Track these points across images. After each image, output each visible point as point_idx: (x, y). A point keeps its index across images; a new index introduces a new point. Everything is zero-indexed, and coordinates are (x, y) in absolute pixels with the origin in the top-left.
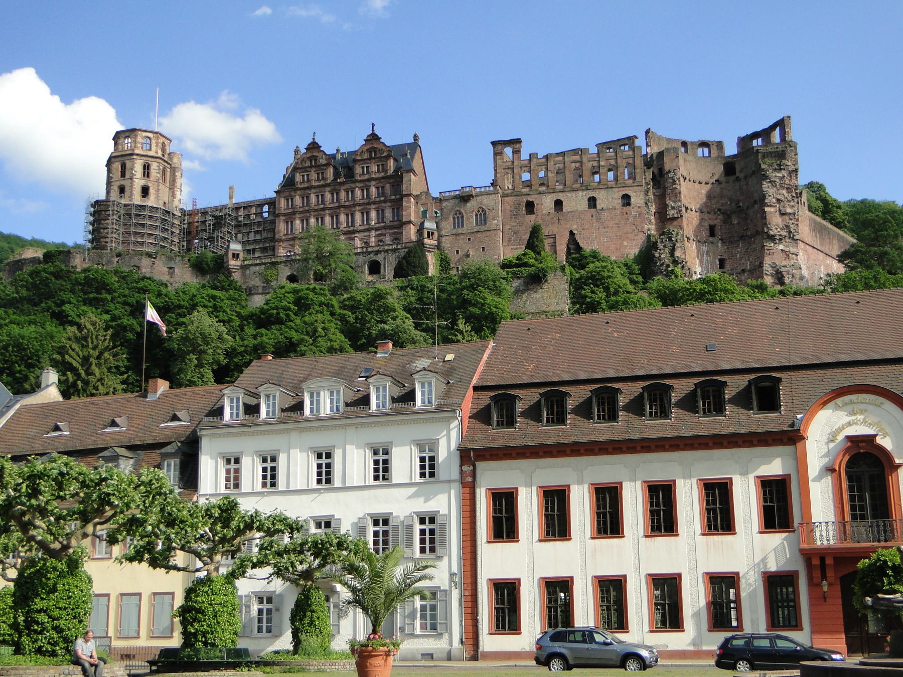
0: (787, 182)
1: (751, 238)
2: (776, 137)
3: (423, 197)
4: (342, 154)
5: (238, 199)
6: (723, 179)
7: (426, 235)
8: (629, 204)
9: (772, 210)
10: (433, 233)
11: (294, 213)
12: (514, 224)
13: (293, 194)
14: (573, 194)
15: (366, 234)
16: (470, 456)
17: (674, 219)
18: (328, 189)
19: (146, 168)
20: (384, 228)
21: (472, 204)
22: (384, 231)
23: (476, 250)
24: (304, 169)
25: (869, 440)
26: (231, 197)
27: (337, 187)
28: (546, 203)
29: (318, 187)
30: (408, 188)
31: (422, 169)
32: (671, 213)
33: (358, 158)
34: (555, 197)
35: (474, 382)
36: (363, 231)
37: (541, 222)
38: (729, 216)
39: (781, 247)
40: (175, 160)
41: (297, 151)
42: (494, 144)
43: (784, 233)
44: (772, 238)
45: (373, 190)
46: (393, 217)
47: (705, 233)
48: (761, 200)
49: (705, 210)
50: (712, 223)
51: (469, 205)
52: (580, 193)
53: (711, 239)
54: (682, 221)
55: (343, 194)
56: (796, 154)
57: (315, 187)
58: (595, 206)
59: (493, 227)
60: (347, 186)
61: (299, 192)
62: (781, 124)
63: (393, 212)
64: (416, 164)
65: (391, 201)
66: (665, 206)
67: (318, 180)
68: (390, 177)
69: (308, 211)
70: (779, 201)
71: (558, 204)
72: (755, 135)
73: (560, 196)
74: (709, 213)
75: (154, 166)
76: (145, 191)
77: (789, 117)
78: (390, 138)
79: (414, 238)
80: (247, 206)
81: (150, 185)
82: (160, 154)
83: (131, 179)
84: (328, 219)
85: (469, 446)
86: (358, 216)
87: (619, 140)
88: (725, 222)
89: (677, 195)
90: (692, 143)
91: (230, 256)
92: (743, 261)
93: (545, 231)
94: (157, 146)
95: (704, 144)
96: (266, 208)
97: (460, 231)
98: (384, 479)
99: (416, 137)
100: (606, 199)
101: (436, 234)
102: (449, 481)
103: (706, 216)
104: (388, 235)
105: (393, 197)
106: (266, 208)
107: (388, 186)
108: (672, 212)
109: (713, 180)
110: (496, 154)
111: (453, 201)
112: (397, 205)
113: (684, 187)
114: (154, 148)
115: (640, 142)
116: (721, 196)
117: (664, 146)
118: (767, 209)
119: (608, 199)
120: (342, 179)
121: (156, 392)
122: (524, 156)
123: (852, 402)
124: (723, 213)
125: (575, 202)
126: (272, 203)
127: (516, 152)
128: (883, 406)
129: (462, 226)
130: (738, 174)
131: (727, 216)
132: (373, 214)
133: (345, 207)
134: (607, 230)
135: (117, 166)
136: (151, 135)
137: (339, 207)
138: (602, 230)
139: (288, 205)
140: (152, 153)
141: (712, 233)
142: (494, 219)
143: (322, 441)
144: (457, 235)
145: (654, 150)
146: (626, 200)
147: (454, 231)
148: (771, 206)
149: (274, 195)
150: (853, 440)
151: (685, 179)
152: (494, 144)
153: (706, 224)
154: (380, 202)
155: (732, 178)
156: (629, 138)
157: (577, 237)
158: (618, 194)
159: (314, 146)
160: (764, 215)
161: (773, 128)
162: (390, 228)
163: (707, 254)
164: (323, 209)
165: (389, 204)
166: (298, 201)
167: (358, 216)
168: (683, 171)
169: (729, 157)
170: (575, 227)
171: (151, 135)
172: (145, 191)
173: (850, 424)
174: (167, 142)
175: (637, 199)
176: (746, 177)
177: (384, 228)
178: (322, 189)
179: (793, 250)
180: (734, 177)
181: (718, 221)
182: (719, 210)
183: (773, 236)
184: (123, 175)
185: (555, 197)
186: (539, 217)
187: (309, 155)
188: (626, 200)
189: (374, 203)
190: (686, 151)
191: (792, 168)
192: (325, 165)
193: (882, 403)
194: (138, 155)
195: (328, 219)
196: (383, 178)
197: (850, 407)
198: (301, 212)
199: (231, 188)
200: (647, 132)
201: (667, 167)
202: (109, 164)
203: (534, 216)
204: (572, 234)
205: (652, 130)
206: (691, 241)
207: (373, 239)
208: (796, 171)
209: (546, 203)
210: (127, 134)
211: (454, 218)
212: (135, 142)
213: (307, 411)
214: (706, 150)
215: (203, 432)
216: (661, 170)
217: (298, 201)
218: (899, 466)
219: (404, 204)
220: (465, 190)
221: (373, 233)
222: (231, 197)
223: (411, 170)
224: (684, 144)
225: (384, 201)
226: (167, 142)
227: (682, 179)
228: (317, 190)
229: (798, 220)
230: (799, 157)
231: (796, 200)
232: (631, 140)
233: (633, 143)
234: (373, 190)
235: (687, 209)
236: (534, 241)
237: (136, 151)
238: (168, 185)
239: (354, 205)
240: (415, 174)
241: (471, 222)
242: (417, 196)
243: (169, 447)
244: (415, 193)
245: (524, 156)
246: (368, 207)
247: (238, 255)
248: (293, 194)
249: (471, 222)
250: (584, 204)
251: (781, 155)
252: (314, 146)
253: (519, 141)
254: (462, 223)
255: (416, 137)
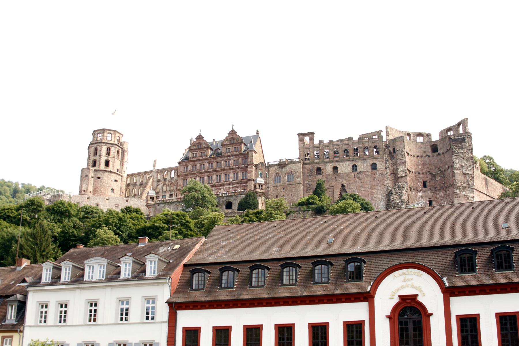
0: (467, 156)
1: (446, 188)
2: (461, 131)
3: (260, 165)
4: (216, 142)
5: (159, 167)
6: (430, 154)
7: (258, 187)
8: (376, 169)
9: (458, 172)
10: (262, 186)
11: (187, 175)
12: (309, 180)
13: (188, 164)
14: (344, 163)
15: (227, 186)
16: (174, 307)
17: (402, 177)
18: (206, 161)
19: (108, 150)
20: (238, 183)
21: (286, 169)
22: (237, 185)
23: (288, 195)
24: (194, 150)
25: (413, 298)
26: (154, 166)
27: (212, 160)
28: (328, 168)
29: (202, 160)
30: (252, 160)
31: (261, 150)
32: (400, 173)
33: (225, 143)
34: (333, 165)
35: (185, 261)
36: (227, 185)
37: (325, 179)
38: (434, 176)
39: (464, 193)
40: (125, 146)
41: (191, 140)
42: (299, 135)
43: (465, 185)
44: (458, 187)
45: (232, 161)
46: (243, 177)
47: (420, 185)
48: (452, 167)
49: (421, 172)
50: (425, 180)
51: (284, 170)
52: (348, 163)
53: (424, 189)
54: (407, 179)
55: (215, 164)
56: (471, 140)
57: (199, 160)
58: (356, 170)
59: (298, 182)
60: (218, 159)
61: (191, 163)
62: (463, 123)
63: (243, 174)
64: (256, 148)
65: (242, 168)
66: (397, 169)
67: (202, 156)
68: (242, 154)
69: (195, 174)
70: (462, 166)
71: (335, 169)
72: (449, 129)
73: (337, 164)
74: (423, 174)
75: (112, 149)
76: (107, 163)
77: (467, 119)
78: (242, 133)
79: (253, 187)
80: (161, 171)
81: (110, 159)
82: (116, 142)
83: (100, 156)
84: (206, 178)
85: (174, 300)
86: (223, 176)
87: (372, 133)
88: (432, 179)
89: (404, 163)
90: (414, 134)
91: (149, 198)
92: (443, 202)
93: (326, 185)
94: (115, 138)
95: (420, 135)
96: (173, 172)
97: (278, 184)
98: (126, 320)
99: (258, 132)
100: (362, 166)
101: (264, 187)
102: (161, 322)
103: (421, 176)
104: (239, 187)
105: (243, 166)
106: (173, 172)
107: (240, 159)
108: (401, 173)
109: (424, 155)
110: (300, 141)
111: (275, 168)
112: (245, 170)
113: (407, 159)
114: (113, 139)
115: (384, 134)
116: (430, 164)
117: (397, 135)
118: (455, 171)
119: (363, 166)
120: (215, 156)
121: (21, 266)
122: (316, 141)
123: (403, 274)
124: (431, 174)
125: (345, 167)
126: (176, 169)
127: (312, 139)
128: (422, 276)
129: (280, 182)
130: (439, 152)
131: (433, 176)
132: (232, 175)
133: (216, 171)
134: (363, 184)
135: (93, 149)
136: (112, 132)
137: (213, 171)
138: (361, 184)
139: (184, 170)
140: (112, 142)
141: (425, 185)
142: (298, 178)
143: (92, 295)
144: (277, 186)
145: (391, 138)
146: (374, 166)
147: (275, 185)
148: (457, 169)
149: (177, 165)
150: (403, 298)
151: (408, 154)
152: (299, 135)
153: (421, 180)
154: (236, 168)
155: (435, 154)
156: (378, 132)
157: (346, 188)
158: (369, 163)
159: (200, 137)
160: (454, 176)
161: (459, 124)
162: (241, 183)
163: (422, 198)
164: (204, 173)
165: (240, 170)
166: (190, 168)
167: (223, 176)
168: (407, 149)
169: (434, 142)
170: (345, 182)
171: (112, 132)
172: (107, 163)
173: (402, 287)
174: (120, 136)
175: (380, 166)
176: (443, 153)
177: (238, 183)
178: (204, 161)
179: (471, 195)
180: (437, 153)
181: (428, 179)
182: (429, 172)
183: (459, 186)
184: (96, 154)
185: (333, 165)
186: (324, 177)
187: (197, 142)
188: (374, 166)
189: (232, 169)
190: (410, 139)
191: (469, 148)
192: (205, 148)
193: (421, 275)
194: (104, 143)
195: (206, 178)
196: (238, 155)
197: (402, 277)
198: (191, 174)
199: (155, 161)
200: (387, 128)
201: (398, 148)
202: (89, 148)
203: (321, 176)
204: (343, 186)
205: (390, 126)
206: (412, 190)
207: (231, 189)
208: (472, 149)
209: (328, 168)
210: (99, 132)
211: (275, 177)
212: (103, 136)
213: (86, 278)
214: (422, 138)
215: (29, 289)
216: (394, 149)
217: (190, 168)
218: (432, 314)
219: (249, 169)
220: (282, 161)
221: (231, 186)
222: (154, 166)
223: (253, 151)
224: (409, 134)
225: (238, 168)
226: (120, 136)
227: (406, 154)
228: (201, 162)
229: (473, 178)
230: (473, 141)
231: (472, 166)
232: (379, 133)
233: (380, 134)
234: (232, 161)
235: (409, 171)
236: (318, 190)
237: (103, 141)
238: (120, 159)
239: (221, 170)
240: (255, 152)
241: (285, 179)
242: (257, 165)
243: (12, 297)
244: (256, 163)
245: (316, 141)
246: (229, 171)
247: (153, 198)
248: (188, 164)
249: (285, 179)
250: (349, 169)
251: (463, 140)
252: (200, 137)
253: (313, 133)
254: (280, 180)
255: (258, 132)
